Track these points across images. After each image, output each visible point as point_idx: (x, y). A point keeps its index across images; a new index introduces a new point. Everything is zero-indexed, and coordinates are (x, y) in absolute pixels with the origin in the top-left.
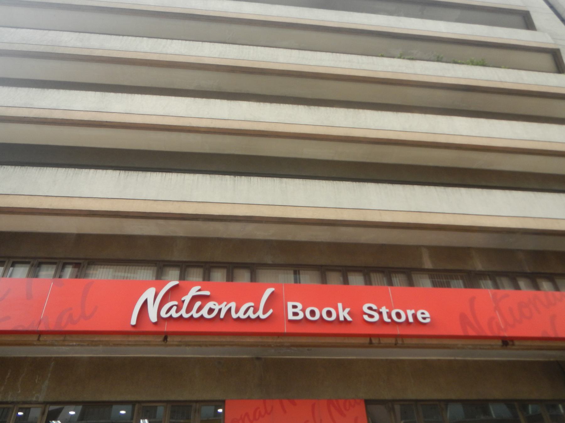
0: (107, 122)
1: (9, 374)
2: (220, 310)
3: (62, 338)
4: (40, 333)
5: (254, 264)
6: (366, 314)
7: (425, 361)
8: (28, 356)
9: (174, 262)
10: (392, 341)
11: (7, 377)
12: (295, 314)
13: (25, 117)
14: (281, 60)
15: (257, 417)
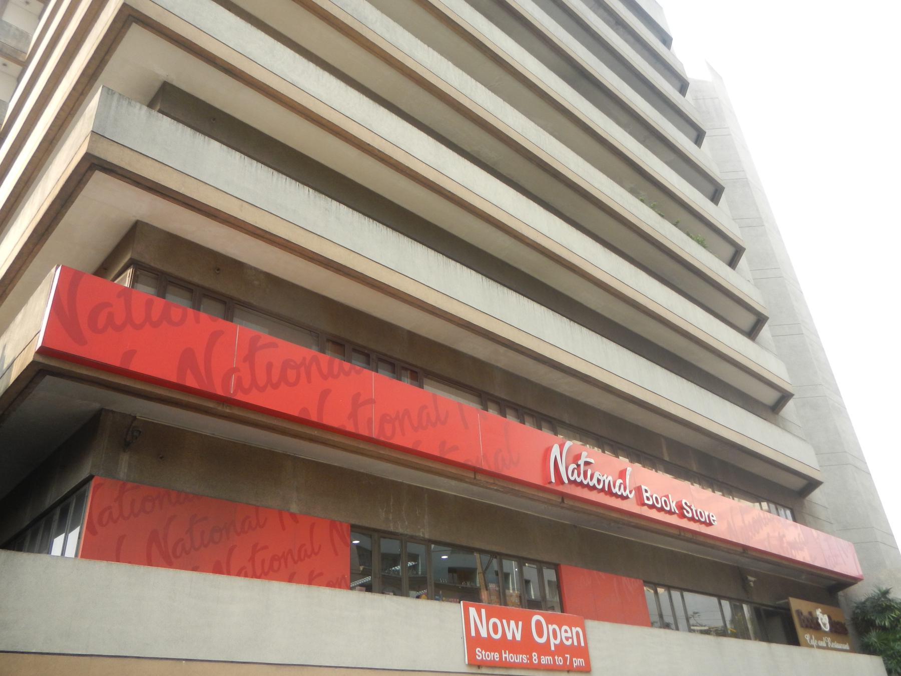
0: (450, 192)
1: (392, 500)
2: (604, 481)
3: (492, 481)
4: (476, 470)
5: (555, 419)
7: (672, 551)
9: (496, 397)
10: (676, 532)
11: (391, 503)
13: (369, 144)
14: (572, 167)
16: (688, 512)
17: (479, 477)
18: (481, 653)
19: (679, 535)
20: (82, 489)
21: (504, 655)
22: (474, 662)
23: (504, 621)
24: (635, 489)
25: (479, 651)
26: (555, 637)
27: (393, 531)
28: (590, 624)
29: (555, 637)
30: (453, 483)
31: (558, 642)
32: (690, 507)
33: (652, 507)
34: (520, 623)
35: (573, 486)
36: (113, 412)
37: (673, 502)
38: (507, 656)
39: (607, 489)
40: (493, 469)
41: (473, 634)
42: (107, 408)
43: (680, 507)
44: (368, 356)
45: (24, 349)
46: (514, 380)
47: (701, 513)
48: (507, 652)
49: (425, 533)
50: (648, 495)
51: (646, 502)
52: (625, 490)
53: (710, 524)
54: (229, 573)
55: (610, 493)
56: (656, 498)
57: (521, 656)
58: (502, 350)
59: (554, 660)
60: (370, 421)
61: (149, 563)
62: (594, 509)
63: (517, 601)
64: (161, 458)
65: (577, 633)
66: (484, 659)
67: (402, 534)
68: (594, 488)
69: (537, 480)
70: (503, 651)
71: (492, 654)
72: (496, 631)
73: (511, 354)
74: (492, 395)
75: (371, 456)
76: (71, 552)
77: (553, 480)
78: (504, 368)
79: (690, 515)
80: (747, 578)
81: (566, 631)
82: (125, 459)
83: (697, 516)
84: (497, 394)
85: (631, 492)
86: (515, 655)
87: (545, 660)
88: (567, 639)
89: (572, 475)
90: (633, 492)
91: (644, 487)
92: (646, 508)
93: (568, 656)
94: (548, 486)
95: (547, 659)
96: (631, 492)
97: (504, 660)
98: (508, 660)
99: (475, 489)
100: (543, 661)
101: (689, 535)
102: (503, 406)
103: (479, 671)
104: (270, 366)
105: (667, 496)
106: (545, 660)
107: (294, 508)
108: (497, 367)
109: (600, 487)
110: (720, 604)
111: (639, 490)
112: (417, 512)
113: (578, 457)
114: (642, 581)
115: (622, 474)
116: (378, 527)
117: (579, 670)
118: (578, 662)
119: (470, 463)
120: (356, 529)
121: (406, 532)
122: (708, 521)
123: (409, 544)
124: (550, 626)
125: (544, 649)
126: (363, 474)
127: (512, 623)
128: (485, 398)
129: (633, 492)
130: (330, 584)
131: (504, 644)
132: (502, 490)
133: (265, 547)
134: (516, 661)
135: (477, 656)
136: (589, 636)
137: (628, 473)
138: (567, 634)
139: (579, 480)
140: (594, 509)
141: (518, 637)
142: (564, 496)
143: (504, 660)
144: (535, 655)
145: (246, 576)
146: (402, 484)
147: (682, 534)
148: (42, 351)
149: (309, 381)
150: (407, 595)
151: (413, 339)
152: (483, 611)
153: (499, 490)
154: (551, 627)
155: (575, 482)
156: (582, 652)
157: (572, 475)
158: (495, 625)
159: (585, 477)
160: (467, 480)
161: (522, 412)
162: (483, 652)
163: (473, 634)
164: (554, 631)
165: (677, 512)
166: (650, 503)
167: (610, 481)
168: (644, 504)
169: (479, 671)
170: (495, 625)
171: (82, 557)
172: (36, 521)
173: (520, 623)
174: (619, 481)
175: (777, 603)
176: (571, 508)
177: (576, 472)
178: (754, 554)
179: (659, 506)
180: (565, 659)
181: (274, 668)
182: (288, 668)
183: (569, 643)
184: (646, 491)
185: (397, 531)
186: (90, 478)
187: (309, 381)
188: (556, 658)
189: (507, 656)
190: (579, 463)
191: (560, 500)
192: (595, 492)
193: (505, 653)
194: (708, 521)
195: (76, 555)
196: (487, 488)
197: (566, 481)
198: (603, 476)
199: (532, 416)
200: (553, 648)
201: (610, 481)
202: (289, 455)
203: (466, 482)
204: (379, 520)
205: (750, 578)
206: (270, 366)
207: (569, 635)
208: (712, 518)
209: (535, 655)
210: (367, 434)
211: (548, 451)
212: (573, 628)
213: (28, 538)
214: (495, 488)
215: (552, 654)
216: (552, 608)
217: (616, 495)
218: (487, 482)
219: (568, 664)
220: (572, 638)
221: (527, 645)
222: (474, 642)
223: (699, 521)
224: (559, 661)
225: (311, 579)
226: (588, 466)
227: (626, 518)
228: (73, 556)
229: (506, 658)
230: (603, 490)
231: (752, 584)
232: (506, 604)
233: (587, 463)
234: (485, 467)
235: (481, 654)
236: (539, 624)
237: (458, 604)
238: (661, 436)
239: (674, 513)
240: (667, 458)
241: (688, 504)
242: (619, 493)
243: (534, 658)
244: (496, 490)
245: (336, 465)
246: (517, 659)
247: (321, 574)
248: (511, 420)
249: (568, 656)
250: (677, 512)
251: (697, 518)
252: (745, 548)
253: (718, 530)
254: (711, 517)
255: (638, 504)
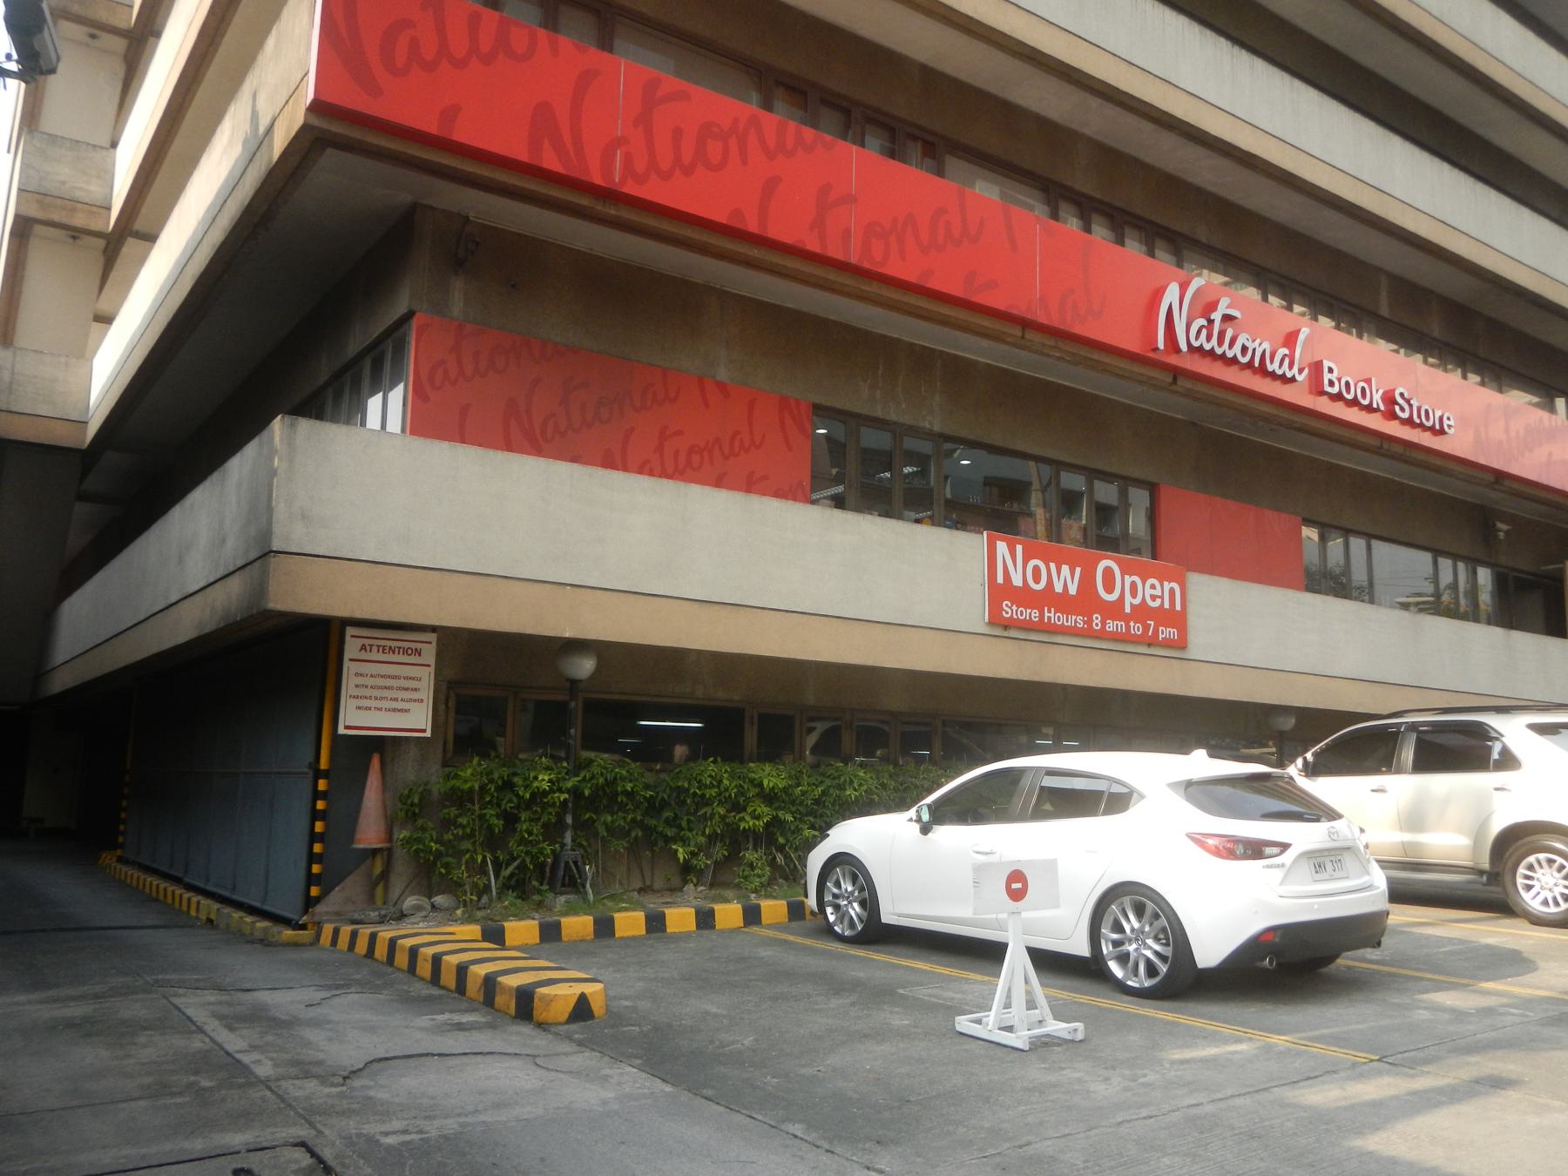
2: (1254, 350)
3: (1051, 342)
4: (1025, 324)
5: (1181, 235)
6: (1398, 404)
8: (903, 338)
10: (1375, 442)
11: (880, 372)
12: (1331, 383)
15: (736, 450)
16: (1402, 409)
17: (1030, 335)
18: (1010, 608)
19: (1379, 448)
20: (402, 330)
21: (1047, 614)
22: (996, 620)
23: (1053, 566)
24: (1310, 366)
25: (1007, 605)
26: (1134, 594)
27: (881, 417)
28: (1196, 580)
29: (1134, 594)
30: (985, 343)
31: (1137, 601)
32: (1408, 401)
33: (1338, 397)
34: (1078, 570)
35: (1196, 356)
36: (431, 208)
37: (1377, 391)
38: (1051, 615)
39: (1257, 364)
40: (1054, 321)
41: (1000, 580)
42: (425, 202)
43: (1390, 399)
44: (847, 112)
45: (287, 102)
46: (1111, 159)
47: (1427, 412)
48: (1053, 609)
49: (934, 422)
50: (1334, 377)
51: (1328, 389)
52: (1291, 366)
53: (1442, 432)
54: (625, 469)
55: (1263, 371)
56: (1347, 384)
57: (1074, 617)
58: (1095, 102)
59: (1128, 627)
60: (847, 232)
61: (509, 446)
62: (1230, 397)
63: (1078, 537)
64: (513, 286)
65: (1172, 592)
66: (1015, 617)
67: (895, 423)
68: (1234, 361)
69: (1131, 343)
70: (1046, 609)
71: (1028, 611)
72: (1037, 579)
73: (1112, 111)
74: (1070, 189)
75: (848, 295)
76: (394, 425)
77: (1161, 345)
78: (1096, 137)
79: (1405, 415)
80: (1495, 525)
81: (1153, 587)
82: (458, 285)
83: (1419, 416)
84: (1077, 187)
85: (1301, 371)
86: (1065, 616)
87: (1111, 626)
88: (1153, 598)
89: (1197, 338)
90: (1306, 372)
91: (1326, 364)
92: (1325, 399)
93: (1152, 623)
94: (1151, 355)
95: (1117, 624)
96: (1301, 371)
97: (1046, 621)
98: (1053, 621)
99: (1024, 353)
100: (1109, 627)
101: (1398, 449)
102: (1088, 208)
103: (1006, 634)
104: (678, 133)
105: (1368, 381)
106: (1111, 626)
107: (722, 374)
108: (1082, 136)
109: (1245, 360)
110: (1435, 563)
111: (1317, 368)
112: (923, 389)
113: (1213, 306)
114: (1300, 519)
115: (1290, 340)
116: (857, 410)
117: (1168, 644)
118: (1167, 632)
119: (1015, 312)
120: (822, 412)
121: (901, 420)
122: (1437, 427)
123: (905, 438)
124: (1127, 577)
125: (1115, 610)
126: (835, 323)
127: (1065, 569)
128: (1056, 194)
129: (1306, 372)
130: (780, 494)
131: (1049, 598)
132: (1069, 359)
133: (679, 433)
134: (1066, 624)
135: (1004, 613)
136: (1191, 596)
137: (1301, 337)
138: (1153, 591)
139: (1207, 347)
140: (1230, 397)
141: (1073, 590)
142: (1177, 373)
143: (1046, 621)
144: (1097, 619)
145: (651, 474)
146: (899, 341)
147: (1386, 446)
148: (316, 107)
149: (745, 163)
150: (900, 517)
151: (931, 80)
152: (1019, 548)
153: (1064, 359)
154: (1128, 580)
155: (1201, 348)
156: (1177, 619)
157: (1197, 338)
158: (1036, 570)
159: (1220, 342)
160: (1009, 339)
161: (1122, 221)
162: (1014, 608)
163: (1000, 580)
164: (1133, 585)
165: (1382, 407)
166: (1335, 390)
167: (1264, 351)
168: (1322, 393)
169: (1006, 634)
170: (1036, 570)
171: (413, 433)
172: (337, 376)
173: (1078, 570)
174: (1284, 351)
175: (1543, 568)
176: (1188, 394)
177: (1204, 332)
178: (1516, 486)
179: (1350, 397)
180: (1146, 628)
181: (696, 605)
182: (716, 607)
183: (1157, 603)
184: (1331, 370)
185: (888, 418)
186: (410, 315)
187: (745, 163)
188: (1132, 624)
189: (1051, 615)
190: (1212, 318)
191: (1169, 379)
192: (1235, 368)
193: (1049, 612)
194: (1437, 427)
195: (403, 430)
196: (1043, 354)
197: (1184, 347)
198: (1253, 341)
199: (1139, 228)
200: (1128, 610)
201: (1264, 351)
202: (714, 288)
203: (1007, 343)
204: (858, 397)
205: (1500, 525)
206: (678, 133)
207: (1158, 592)
208: (1446, 422)
209: (1097, 619)
210: (840, 256)
211: (1158, 294)
212: (1166, 583)
213: (330, 401)
214: (1058, 355)
215: (1126, 619)
216: (1138, 552)
217: (1273, 375)
218: (1044, 345)
219: (1150, 634)
220: (1162, 597)
221: (1086, 601)
222: (1000, 592)
223: (1421, 426)
224: (1136, 628)
225: (751, 485)
226: (1228, 324)
227: (1284, 414)
228: (398, 430)
229: (1049, 618)
230: (1250, 365)
231: (1501, 535)
232: (1059, 541)
233: (1227, 318)
234: (1042, 319)
235: (1009, 610)
236: (1108, 573)
237: (979, 536)
238: (1379, 270)
239: (1377, 410)
240: (1384, 311)
241: (1406, 395)
242: (1280, 372)
243: (1096, 621)
244: (1059, 359)
245: (790, 305)
246: (1067, 621)
247: (765, 478)
248: (1101, 232)
249: (1152, 623)
250: (1382, 407)
251: (1418, 421)
252: (1500, 476)
253: (1457, 443)
254: (1445, 419)
255: (1311, 393)
